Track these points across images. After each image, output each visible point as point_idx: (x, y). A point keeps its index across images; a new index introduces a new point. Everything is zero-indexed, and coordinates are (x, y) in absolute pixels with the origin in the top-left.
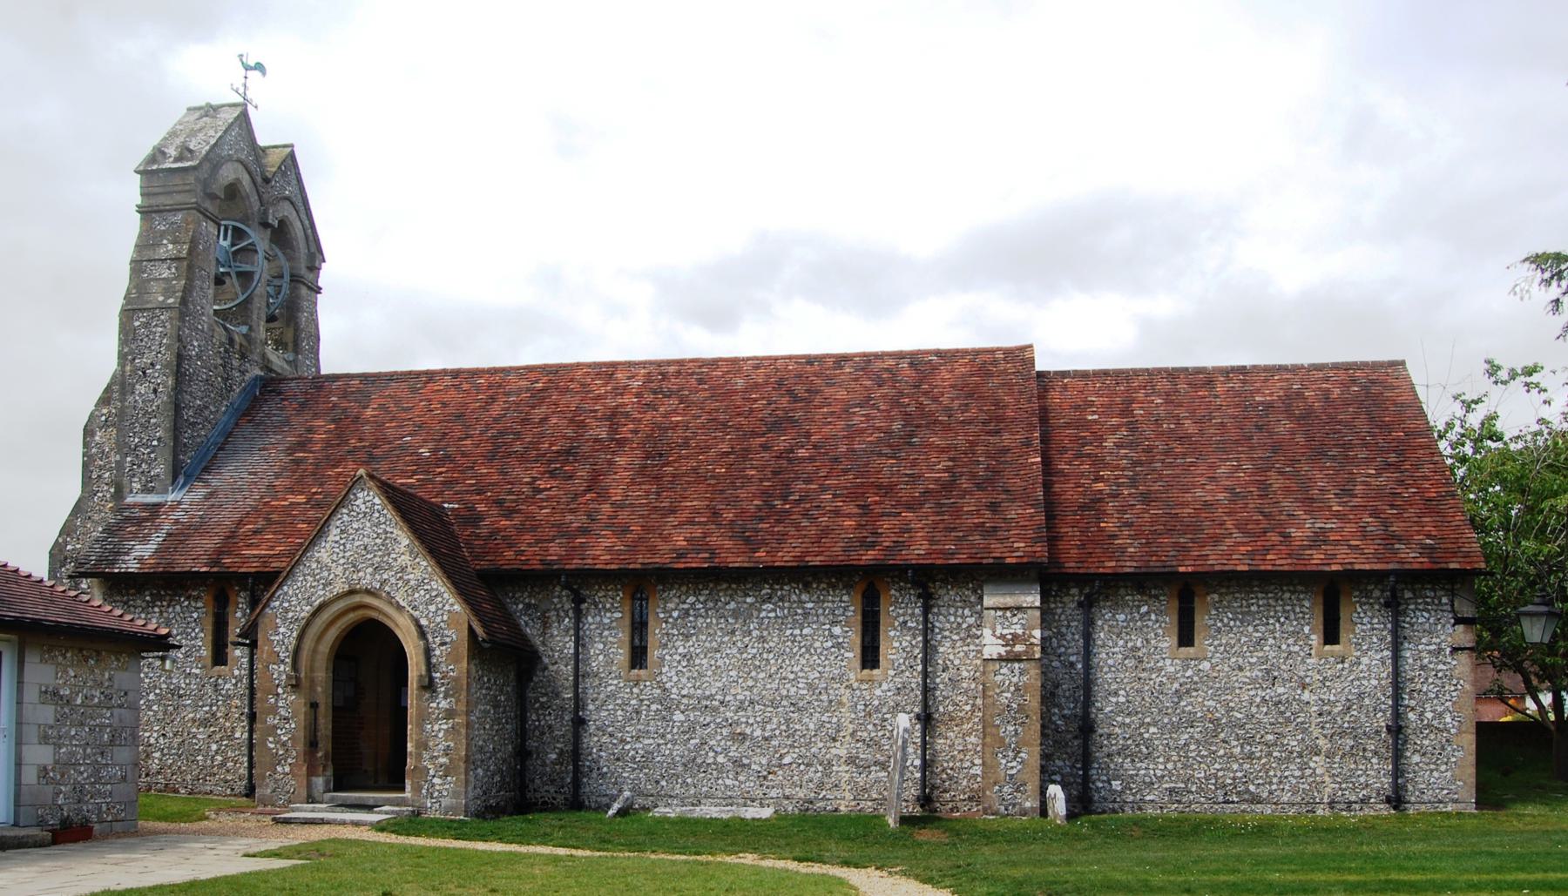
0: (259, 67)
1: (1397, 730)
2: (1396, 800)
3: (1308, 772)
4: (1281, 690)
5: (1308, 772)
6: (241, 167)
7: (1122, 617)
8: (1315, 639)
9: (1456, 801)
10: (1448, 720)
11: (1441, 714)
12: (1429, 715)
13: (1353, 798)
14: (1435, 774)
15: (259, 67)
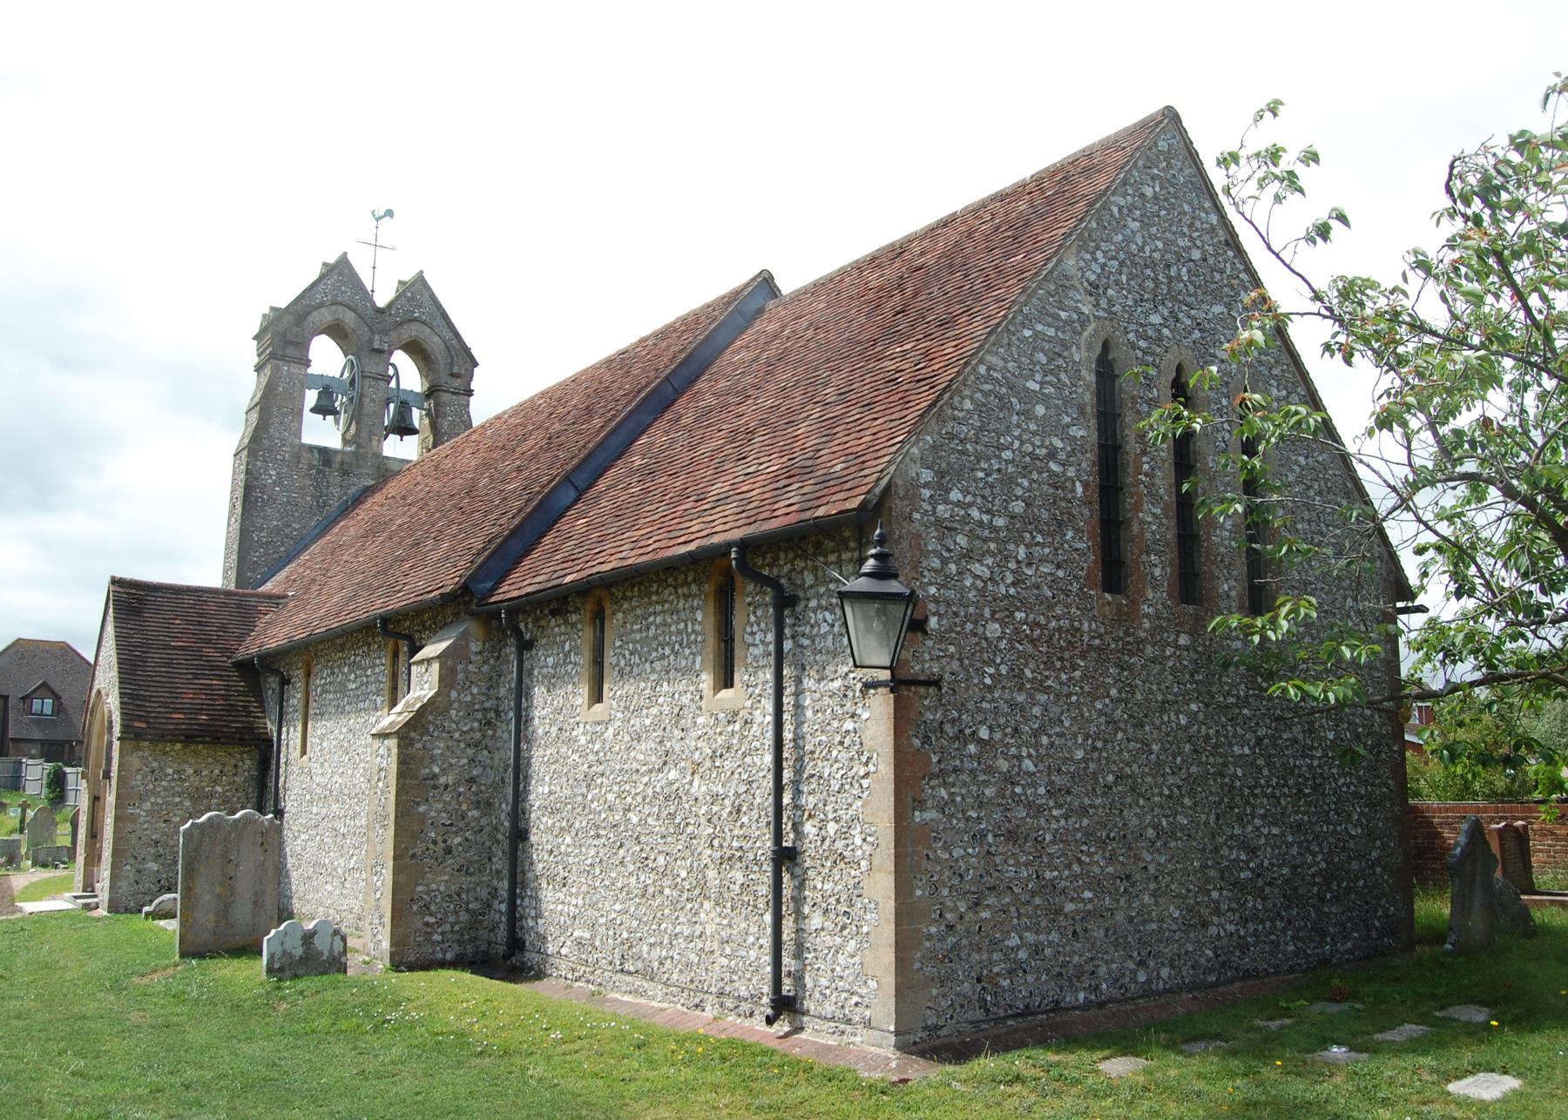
0: (389, 213)
1: (785, 857)
2: (785, 1006)
3: (698, 928)
4: (672, 775)
5: (698, 928)
6: (341, 308)
7: (550, 661)
8: (706, 680)
9: (868, 1024)
10: (858, 841)
11: (844, 834)
12: (832, 828)
13: (743, 992)
14: (841, 959)
15: (389, 213)
